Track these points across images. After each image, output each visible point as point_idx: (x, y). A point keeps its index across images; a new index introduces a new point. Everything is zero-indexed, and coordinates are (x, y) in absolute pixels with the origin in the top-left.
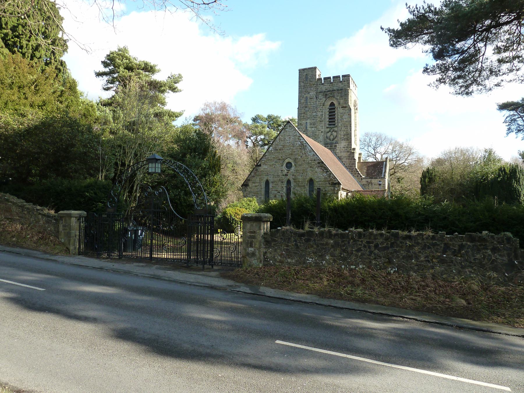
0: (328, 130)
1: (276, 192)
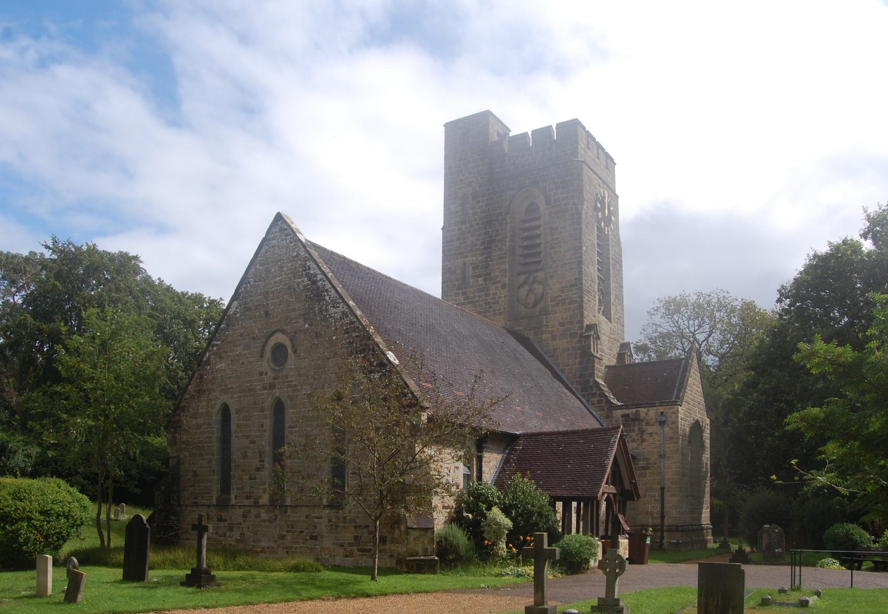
0: (522, 279)
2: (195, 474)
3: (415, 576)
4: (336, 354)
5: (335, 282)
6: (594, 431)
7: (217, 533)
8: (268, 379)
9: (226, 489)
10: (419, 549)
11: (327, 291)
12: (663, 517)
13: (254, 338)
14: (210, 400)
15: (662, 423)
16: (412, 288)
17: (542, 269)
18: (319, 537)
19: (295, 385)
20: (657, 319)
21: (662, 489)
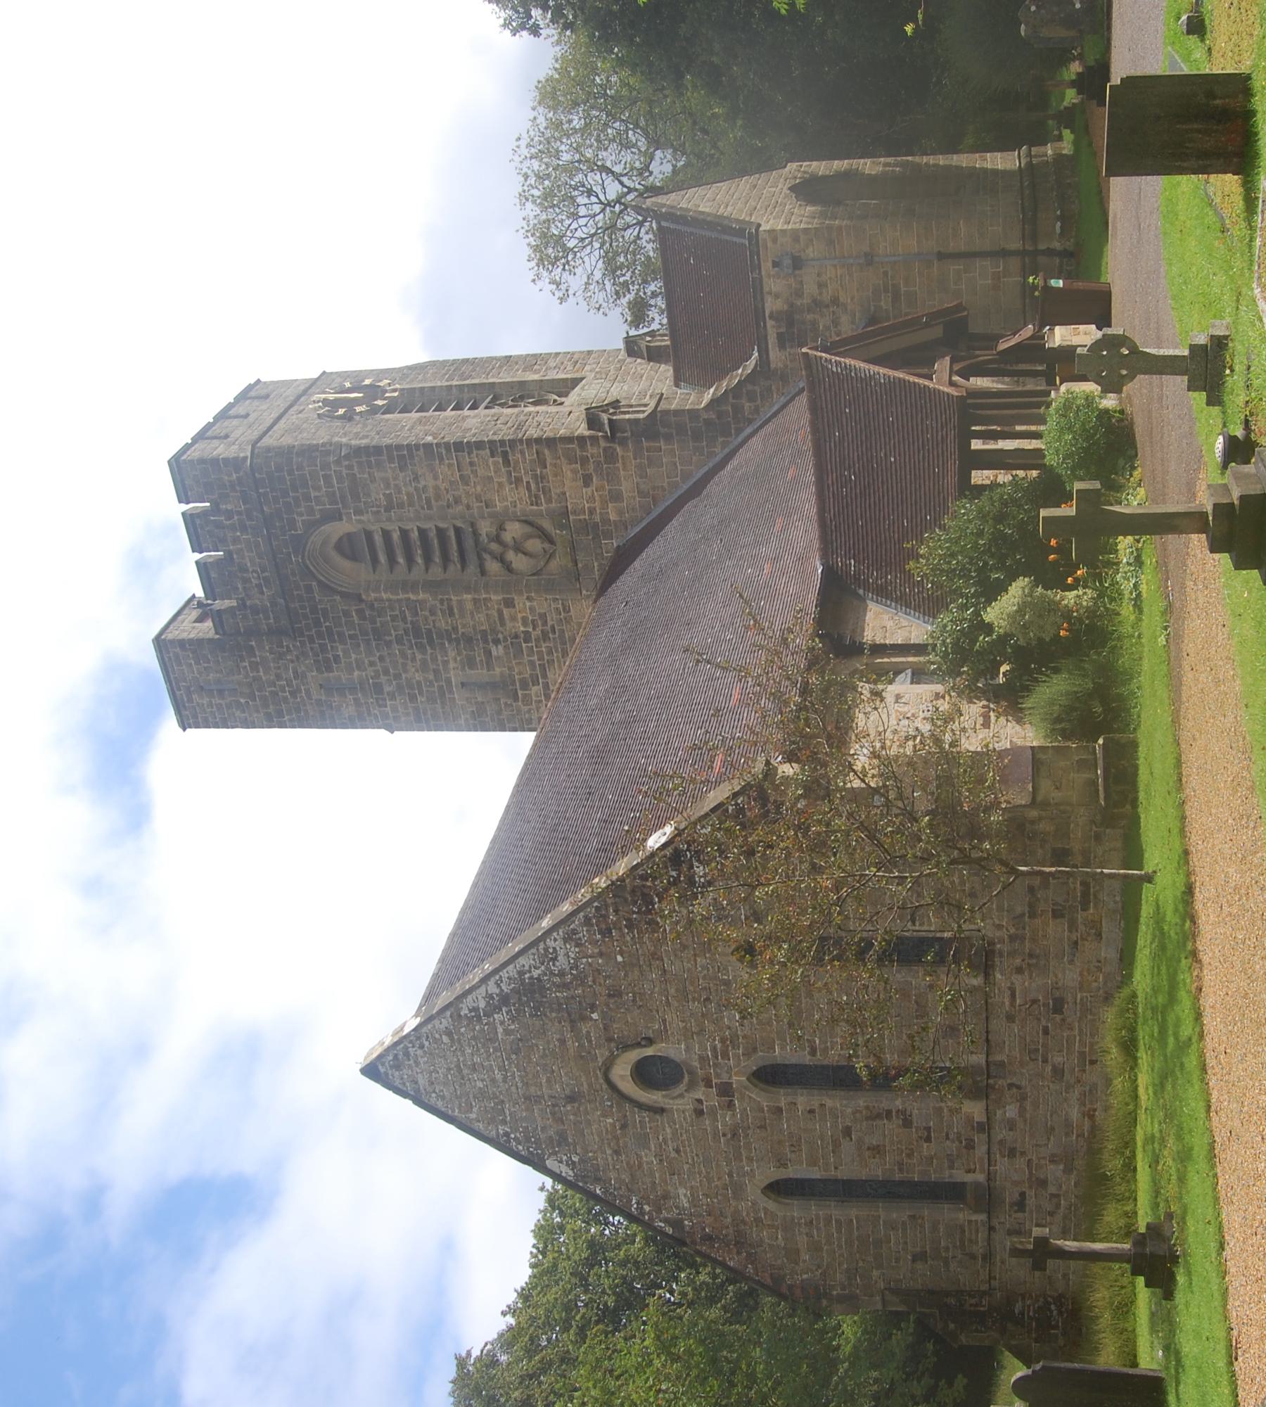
0: (493, 566)
1: (847, 1147)
2: (919, 1257)
3: (1141, 786)
4: (653, 954)
5: (503, 956)
6: (814, 408)
7: (1051, 1214)
8: (712, 1099)
9: (953, 1193)
10: (1081, 777)
11: (521, 973)
12: (1004, 253)
13: (624, 1127)
14: (758, 1220)
15: (797, 263)
16: (513, 795)
17: (473, 525)
18: (1057, 994)
19: (723, 1041)
20: (575, 282)
21: (941, 256)
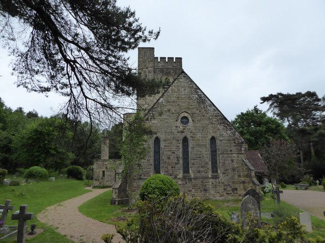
1: (170, 153)
